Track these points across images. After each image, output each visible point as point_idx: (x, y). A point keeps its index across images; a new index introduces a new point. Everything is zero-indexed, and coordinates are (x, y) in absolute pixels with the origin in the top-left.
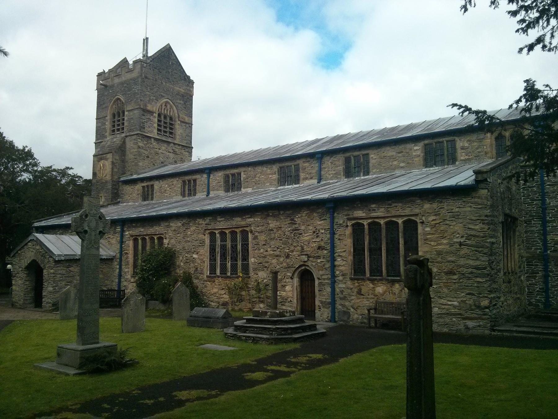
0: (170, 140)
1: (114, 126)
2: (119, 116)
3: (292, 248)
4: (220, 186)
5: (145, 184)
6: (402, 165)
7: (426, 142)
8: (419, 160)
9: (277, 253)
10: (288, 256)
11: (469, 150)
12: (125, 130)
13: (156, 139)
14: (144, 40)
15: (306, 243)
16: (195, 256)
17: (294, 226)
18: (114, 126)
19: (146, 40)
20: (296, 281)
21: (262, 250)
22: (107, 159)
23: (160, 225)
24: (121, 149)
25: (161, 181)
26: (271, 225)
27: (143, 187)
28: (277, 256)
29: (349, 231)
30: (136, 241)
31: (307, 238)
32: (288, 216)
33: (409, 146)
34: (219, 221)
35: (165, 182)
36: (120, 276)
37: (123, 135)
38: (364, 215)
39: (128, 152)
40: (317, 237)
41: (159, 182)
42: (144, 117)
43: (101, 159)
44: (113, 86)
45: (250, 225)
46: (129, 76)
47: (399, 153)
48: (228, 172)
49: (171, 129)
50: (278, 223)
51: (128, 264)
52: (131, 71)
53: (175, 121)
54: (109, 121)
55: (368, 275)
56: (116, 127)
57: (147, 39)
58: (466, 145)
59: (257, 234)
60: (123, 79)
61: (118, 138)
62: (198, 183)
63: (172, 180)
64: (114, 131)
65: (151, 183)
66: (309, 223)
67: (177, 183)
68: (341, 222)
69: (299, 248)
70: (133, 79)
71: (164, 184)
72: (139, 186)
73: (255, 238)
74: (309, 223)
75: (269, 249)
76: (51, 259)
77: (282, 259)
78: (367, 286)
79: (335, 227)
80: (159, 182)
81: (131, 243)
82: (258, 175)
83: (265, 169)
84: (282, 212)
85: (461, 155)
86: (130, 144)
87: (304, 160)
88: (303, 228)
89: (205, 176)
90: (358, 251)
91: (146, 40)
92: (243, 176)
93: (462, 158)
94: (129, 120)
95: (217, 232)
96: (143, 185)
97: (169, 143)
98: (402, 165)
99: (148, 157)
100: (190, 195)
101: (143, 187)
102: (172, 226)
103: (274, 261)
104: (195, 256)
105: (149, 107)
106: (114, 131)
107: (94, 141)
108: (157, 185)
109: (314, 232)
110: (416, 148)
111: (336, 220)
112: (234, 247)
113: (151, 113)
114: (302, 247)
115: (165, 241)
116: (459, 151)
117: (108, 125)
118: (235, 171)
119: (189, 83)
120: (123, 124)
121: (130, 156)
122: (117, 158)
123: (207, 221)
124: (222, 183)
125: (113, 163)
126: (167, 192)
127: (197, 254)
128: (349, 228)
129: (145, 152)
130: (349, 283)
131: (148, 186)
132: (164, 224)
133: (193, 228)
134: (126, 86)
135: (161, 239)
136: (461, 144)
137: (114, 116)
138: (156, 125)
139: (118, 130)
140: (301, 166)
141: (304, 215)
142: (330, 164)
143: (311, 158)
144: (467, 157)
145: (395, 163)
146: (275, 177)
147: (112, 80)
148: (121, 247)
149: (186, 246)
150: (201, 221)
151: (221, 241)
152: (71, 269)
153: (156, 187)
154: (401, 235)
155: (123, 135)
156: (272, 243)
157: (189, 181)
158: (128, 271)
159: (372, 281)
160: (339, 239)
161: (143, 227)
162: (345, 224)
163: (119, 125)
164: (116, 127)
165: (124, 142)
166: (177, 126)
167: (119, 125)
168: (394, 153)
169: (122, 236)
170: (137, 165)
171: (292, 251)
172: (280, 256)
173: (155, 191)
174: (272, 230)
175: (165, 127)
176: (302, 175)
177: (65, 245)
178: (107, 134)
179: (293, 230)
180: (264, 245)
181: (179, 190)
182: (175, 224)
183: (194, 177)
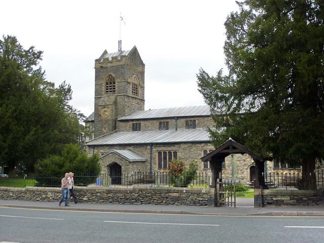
0: (137, 97)
2: (111, 83)
5: (135, 122)
10: (245, 161)
12: (116, 92)
13: (132, 97)
19: (120, 42)
20: (249, 170)
22: (108, 108)
24: (115, 103)
27: (133, 124)
30: (160, 153)
36: (151, 169)
37: (115, 95)
39: (118, 104)
43: (105, 107)
44: (107, 67)
46: (118, 63)
48: (188, 119)
51: (155, 163)
52: (119, 61)
55: (280, 167)
56: (109, 90)
60: (114, 64)
61: (113, 97)
64: (107, 92)
65: (139, 122)
67: (157, 123)
70: (121, 66)
71: (148, 123)
72: (131, 123)
76: (127, 162)
78: (280, 172)
81: (157, 154)
86: (119, 100)
89: (174, 120)
91: (120, 42)
92: (197, 122)
94: (119, 87)
95: (208, 150)
96: (133, 122)
101: (133, 124)
105: (129, 81)
106: (107, 92)
107: (94, 96)
108: (142, 123)
113: (129, 83)
117: (104, 88)
118: (193, 119)
119: (144, 65)
120: (115, 88)
121: (120, 106)
122: (113, 107)
123: (202, 145)
124: (185, 124)
125: (112, 110)
130: (273, 171)
131: (136, 124)
132: (176, 146)
133: (194, 148)
134: (117, 69)
135: (175, 153)
137: (107, 84)
139: (110, 91)
147: (106, 64)
148: (151, 156)
150: (199, 145)
152: (134, 166)
153: (142, 124)
155: (115, 95)
157: (164, 122)
158: (156, 168)
159: (282, 170)
161: (165, 147)
163: (111, 89)
164: (109, 90)
165: (116, 99)
166: (139, 89)
167: (111, 89)
169: (151, 151)
170: (124, 111)
177: (127, 154)
178: (103, 93)
182: (183, 146)
183: (167, 120)
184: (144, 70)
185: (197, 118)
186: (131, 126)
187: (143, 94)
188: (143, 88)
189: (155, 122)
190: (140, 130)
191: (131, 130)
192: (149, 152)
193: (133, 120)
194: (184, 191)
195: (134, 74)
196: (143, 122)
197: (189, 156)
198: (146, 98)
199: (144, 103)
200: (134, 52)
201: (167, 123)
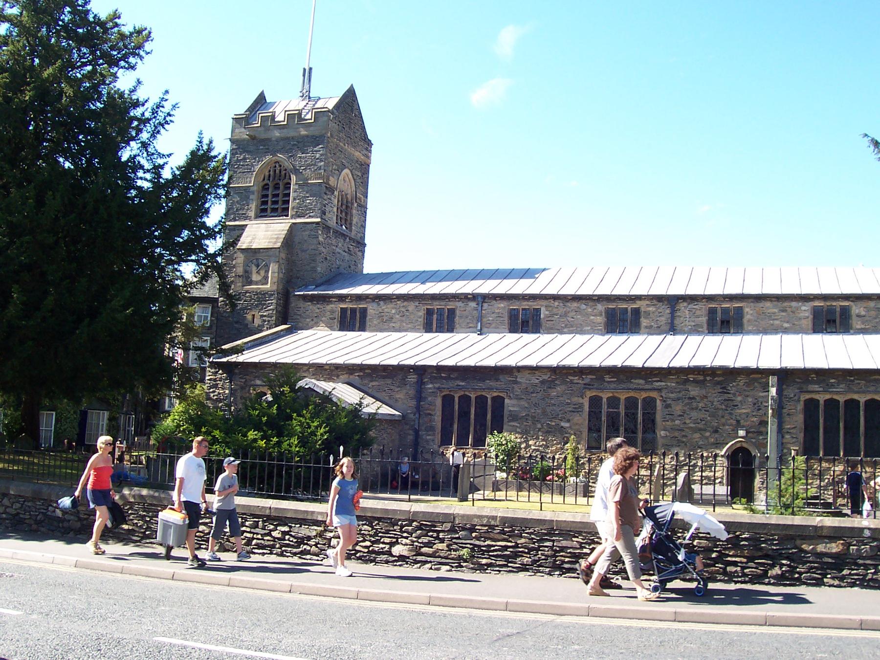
0: (347, 232)
1: (265, 203)
3: (723, 420)
4: (502, 323)
6: (786, 325)
7: (817, 303)
8: (808, 323)
9: (700, 426)
10: (716, 431)
11: (867, 318)
13: (336, 232)
14: (305, 70)
15: (744, 416)
16: (563, 424)
17: (726, 396)
18: (265, 203)
21: (677, 422)
23: (497, 380)
25: (382, 303)
26: (692, 393)
28: (700, 430)
29: (800, 406)
31: (744, 411)
32: (718, 383)
33: (794, 304)
34: (608, 382)
35: (391, 306)
38: (821, 389)
40: (759, 410)
41: (379, 305)
42: (325, 197)
45: (659, 390)
47: (783, 311)
49: (346, 214)
50: (703, 392)
51: (432, 429)
53: (352, 204)
54: (256, 193)
57: (311, 69)
58: (863, 313)
59: (669, 402)
62: (458, 312)
63: (405, 303)
66: (747, 393)
68: (792, 396)
69: (734, 422)
71: (389, 309)
73: (668, 406)
74: (747, 393)
75: (688, 421)
77: (708, 434)
79: (784, 400)
80: (379, 305)
81: (439, 402)
82: (571, 314)
83: (584, 307)
84: (708, 378)
85: (857, 324)
87: (648, 302)
88: (739, 398)
89: (473, 304)
90: (810, 427)
93: (858, 327)
97: (344, 236)
98: (786, 325)
99: (326, 259)
100: (440, 330)
102: (520, 383)
103: (697, 435)
104: (567, 425)
109: (755, 404)
110: (803, 308)
111: (785, 393)
112: (631, 416)
114: (738, 421)
115: (507, 401)
116: (854, 317)
119: (369, 144)
126: (394, 320)
127: (568, 421)
128: (802, 403)
129: (324, 250)
131: (353, 311)
136: (857, 311)
138: (335, 209)
140: (643, 309)
141: (741, 383)
142: (687, 312)
143: (659, 302)
144: (863, 326)
145: (777, 322)
146: (601, 319)
149: (548, 410)
150: (576, 379)
151: (608, 407)
154: (862, 413)
156: (694, 414)
160: (788, 414)
162: (796, 398)
163: (276, 202)
168: (776, 311)
171: (724, 425)
172: (705, 430)
173: (368, 318)
174: (693, 398)
175: (341, 211)
176: (644, 322)
179: (725, 400)
180: (680, 416)
181: (421, 320)
183: (451, 305)
184: (369, 157)
185: (544, 303)
186: (337, 315)
187: (364, 227)
188: (363, 208)
189: (412, 306)
190: (362, 328)
191: (336, 323)
192: (412, 392)
193: (342, 298)
194: (867, 533)
195: (345, 167)
196: (375, 305)
197: (544, 412)
198: (366, 242)
199: (363, 252)
200: (349, 102)
201: (452, 312)
